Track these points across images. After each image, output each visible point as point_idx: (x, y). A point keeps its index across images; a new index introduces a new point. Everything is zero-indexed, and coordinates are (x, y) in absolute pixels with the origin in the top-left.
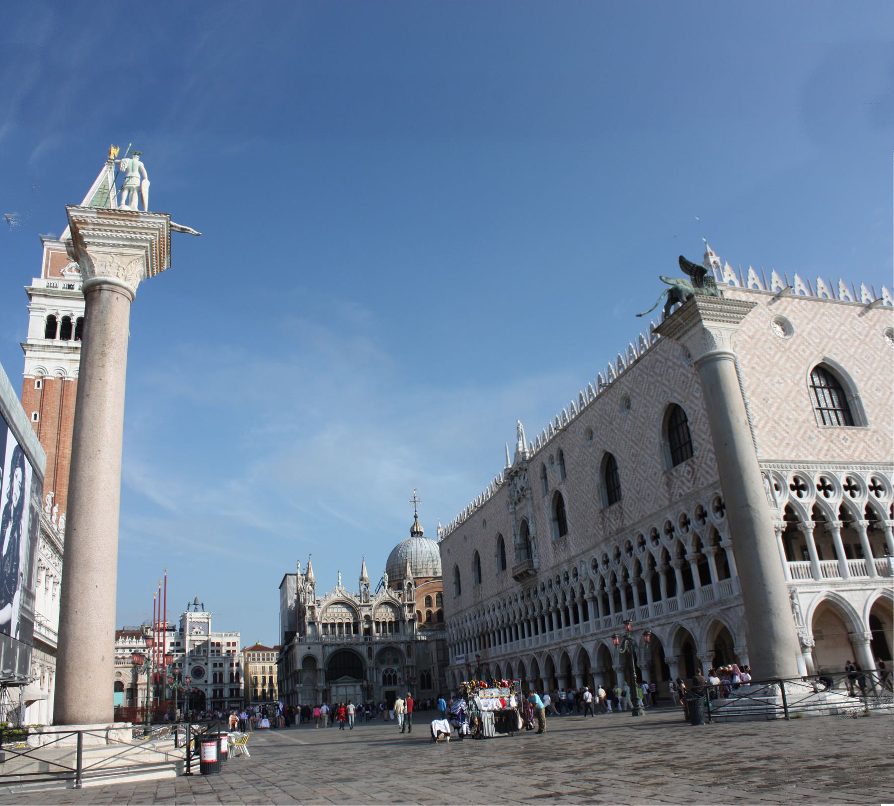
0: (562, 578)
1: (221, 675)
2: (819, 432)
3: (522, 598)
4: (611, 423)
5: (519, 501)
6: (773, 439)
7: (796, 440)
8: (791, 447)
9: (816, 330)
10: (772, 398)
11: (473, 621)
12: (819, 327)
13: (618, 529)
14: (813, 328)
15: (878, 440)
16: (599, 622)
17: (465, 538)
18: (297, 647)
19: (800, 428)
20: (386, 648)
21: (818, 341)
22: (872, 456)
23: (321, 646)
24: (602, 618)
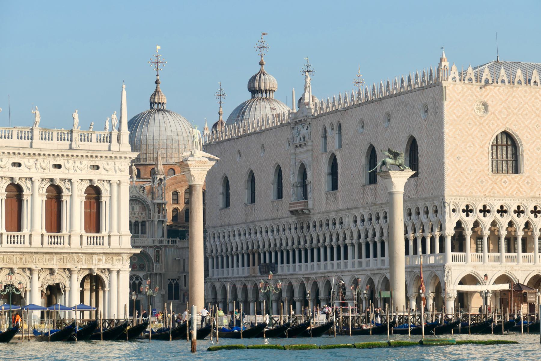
0: (331, 223)
2: (489, 178)
3: (296, 228)
4: (377, 126)
5: (300, 145)
6: (457, 183)
10: (463, 156)
11: (242, 237)
12: (508, 107)
13: (372, 203)
14: (504, 107)
15: (528, 183)
16: (354, 262)
17: (239, 152)
19: (477, 175)
21: (504, 116)
22: (521, 192)
24: (357, 260)
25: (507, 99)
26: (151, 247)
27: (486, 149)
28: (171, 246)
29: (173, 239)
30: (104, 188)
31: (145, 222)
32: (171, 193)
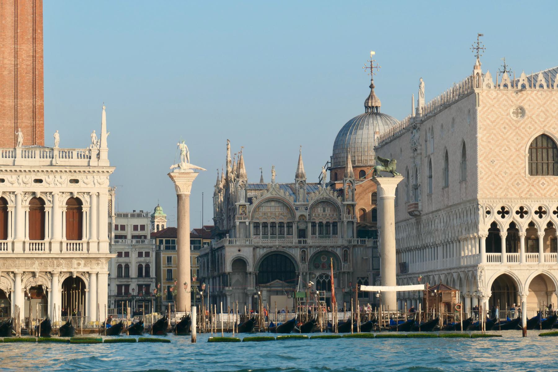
1: (127, 267)
2: (525, 180)
6: (491, 186)
7: (508, 185)
8: (503, 190)
9: (543, 112)
10: (498, 160)
12: (547, 111)
14: (542, 111)
18: (227, 249)
19: (512, 178)
20: (321, 252)
23: (251, 249)
25: (545, 104)
26: (339, 247)
27: (523, 152)
28: (360, 246)
29: (362, 239)
30: (85, 199)
31: (336, 222)
32: (370, 195)
